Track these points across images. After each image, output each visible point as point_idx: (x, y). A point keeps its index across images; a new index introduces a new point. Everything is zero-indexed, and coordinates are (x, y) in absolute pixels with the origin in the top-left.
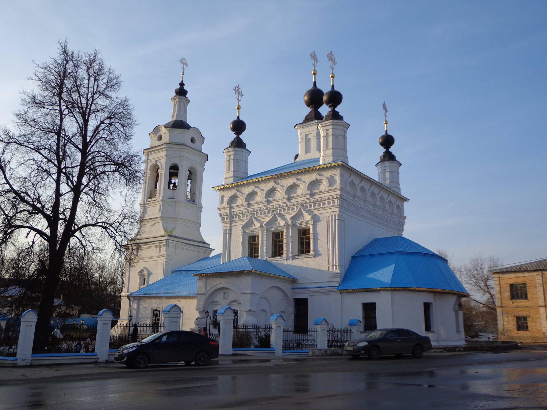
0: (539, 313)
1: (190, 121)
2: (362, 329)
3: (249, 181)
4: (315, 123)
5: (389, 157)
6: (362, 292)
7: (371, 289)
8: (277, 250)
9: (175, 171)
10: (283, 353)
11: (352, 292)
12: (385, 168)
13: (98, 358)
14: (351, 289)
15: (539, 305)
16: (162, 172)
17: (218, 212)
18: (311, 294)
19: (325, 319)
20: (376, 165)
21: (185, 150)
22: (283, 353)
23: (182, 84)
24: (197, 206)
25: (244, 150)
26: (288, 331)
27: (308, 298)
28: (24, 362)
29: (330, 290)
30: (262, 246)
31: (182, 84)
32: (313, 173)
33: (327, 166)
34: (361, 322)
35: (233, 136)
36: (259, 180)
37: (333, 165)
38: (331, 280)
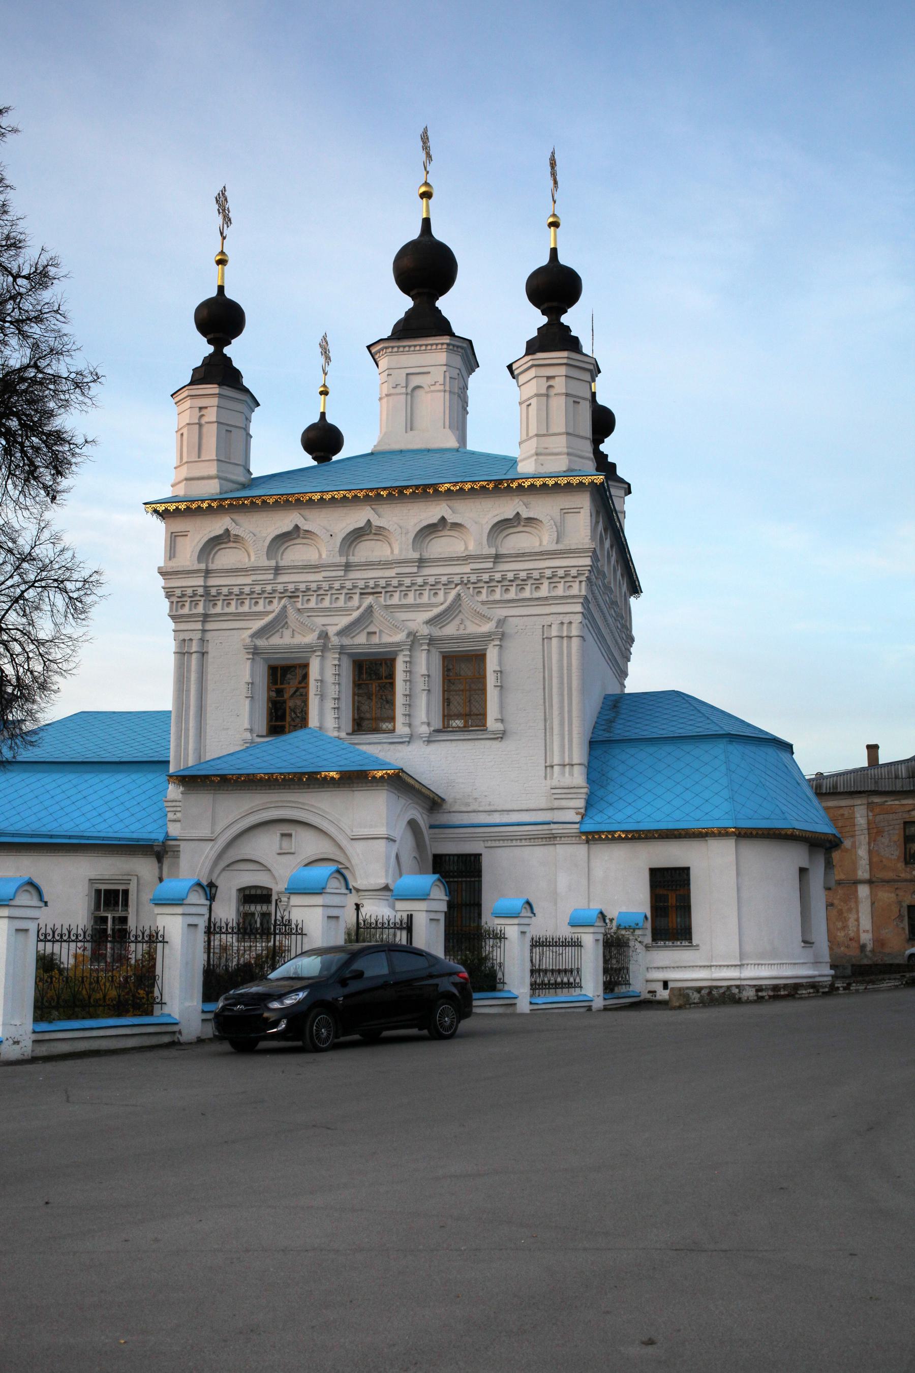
0: (856, 897)
2: (648, 939)
4: (442, 344)
6: (655, 838)
7: (683, 833)
10: (531, 1003)
11: (626, 838)
13: (180, 1032)
14: (623, 831)
15: (859, 877)
17: (161, 582)
18: (489, 844)
22: (531, 1003)
27: (481, 855)
28: (16, 1047)
29: (554, 832)
30: (322, 697)
32: (513, 498)
33: (556, 483)
36: (322, 498)
37: (563, 481)
38: (557, 804)
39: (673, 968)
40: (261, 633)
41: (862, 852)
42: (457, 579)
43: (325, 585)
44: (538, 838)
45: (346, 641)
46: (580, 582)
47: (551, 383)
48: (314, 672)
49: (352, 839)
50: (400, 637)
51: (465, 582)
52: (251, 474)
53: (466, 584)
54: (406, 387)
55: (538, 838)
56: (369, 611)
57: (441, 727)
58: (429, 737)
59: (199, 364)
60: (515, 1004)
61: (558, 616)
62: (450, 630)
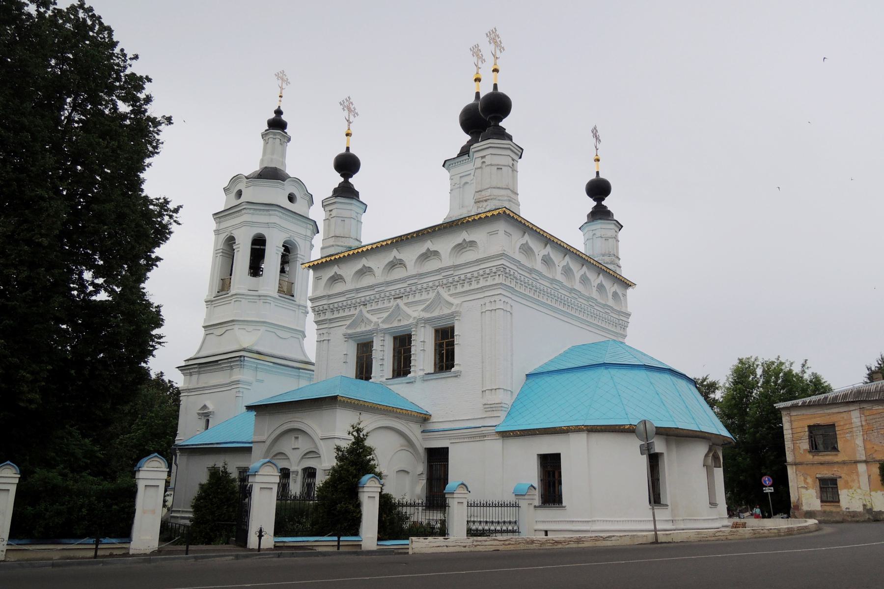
1: (291, 170)
2: (537, 501)
3: (356, 251)
5: (600, 213)
8: (402, 367)
9: (262, 247)
12: (594, 232)
16: (239, 248)
19: (463, 484)
20: (580, 229)
21: (277, 213)
23: (279, 112)
24: (297, 303)
25: (354, 202)
26: (414, 506)
29: (483, 432)
31: (279, 112)
34: (535, 489)
35: (338, 179)
39: (552, 522)
40: (349, 327)
41: (859, 442)
42: (437, 283)
43: (377, 296)
44: (477, 437)
45: (385, 326)
46: (499, 275)
47: (484, 160)
48: (376, 346)
49: (321, 439)
50: (411, 321)
51: (441, 284)
52: (361, 242)
53: (442, 286)
54: (460, 184)
55: (477, 437)
56: (397, 307)
57: (433, 372)
58: (423, 377)
59: (337, 186)
60: (361, 545)
61: (488, 298)
62: (436, 314)
